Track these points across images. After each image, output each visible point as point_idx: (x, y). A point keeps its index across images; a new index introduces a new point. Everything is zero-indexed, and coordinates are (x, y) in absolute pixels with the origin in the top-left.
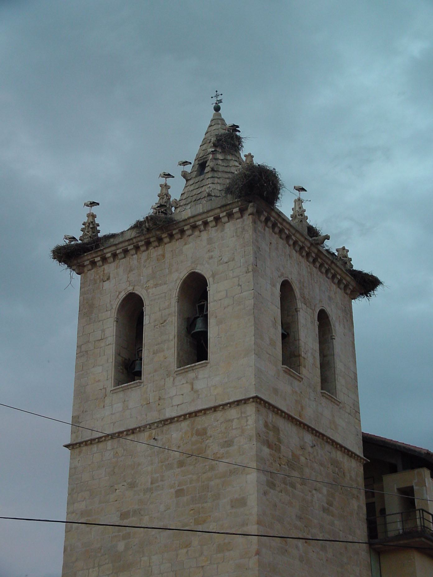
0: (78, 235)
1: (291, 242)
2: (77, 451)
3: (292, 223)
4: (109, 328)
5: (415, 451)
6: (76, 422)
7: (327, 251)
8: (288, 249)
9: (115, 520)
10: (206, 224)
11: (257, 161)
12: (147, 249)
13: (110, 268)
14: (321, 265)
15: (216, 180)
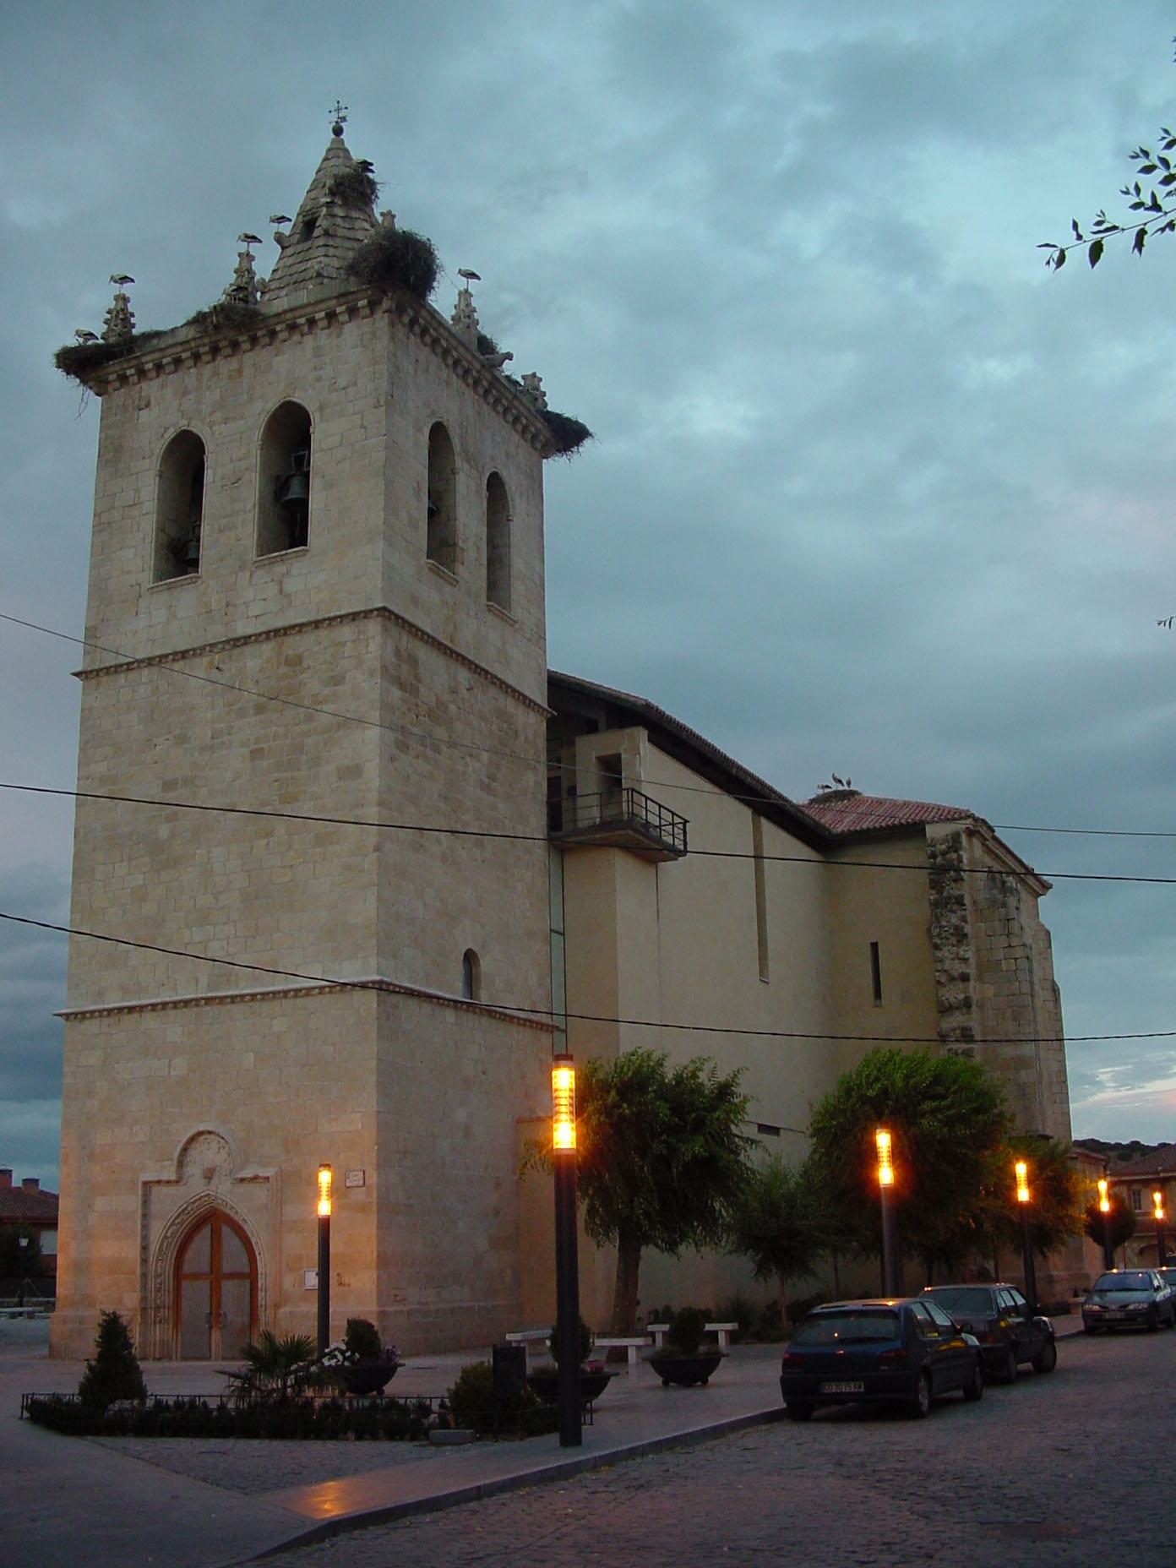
0: (99, 329)
1: (450, 361)
2: (93, 682)
3: (453, 330)
4: (146, 487)
5: (618, 698)
6: (91, 633)
7: (508, 377)
8: (444, 374)
9: (155, 792)
10: (312, 322)
11: (401, 225)
12: (214, 360)
13: (149, 387)
14: (497, 401)
15: (331, 251)
